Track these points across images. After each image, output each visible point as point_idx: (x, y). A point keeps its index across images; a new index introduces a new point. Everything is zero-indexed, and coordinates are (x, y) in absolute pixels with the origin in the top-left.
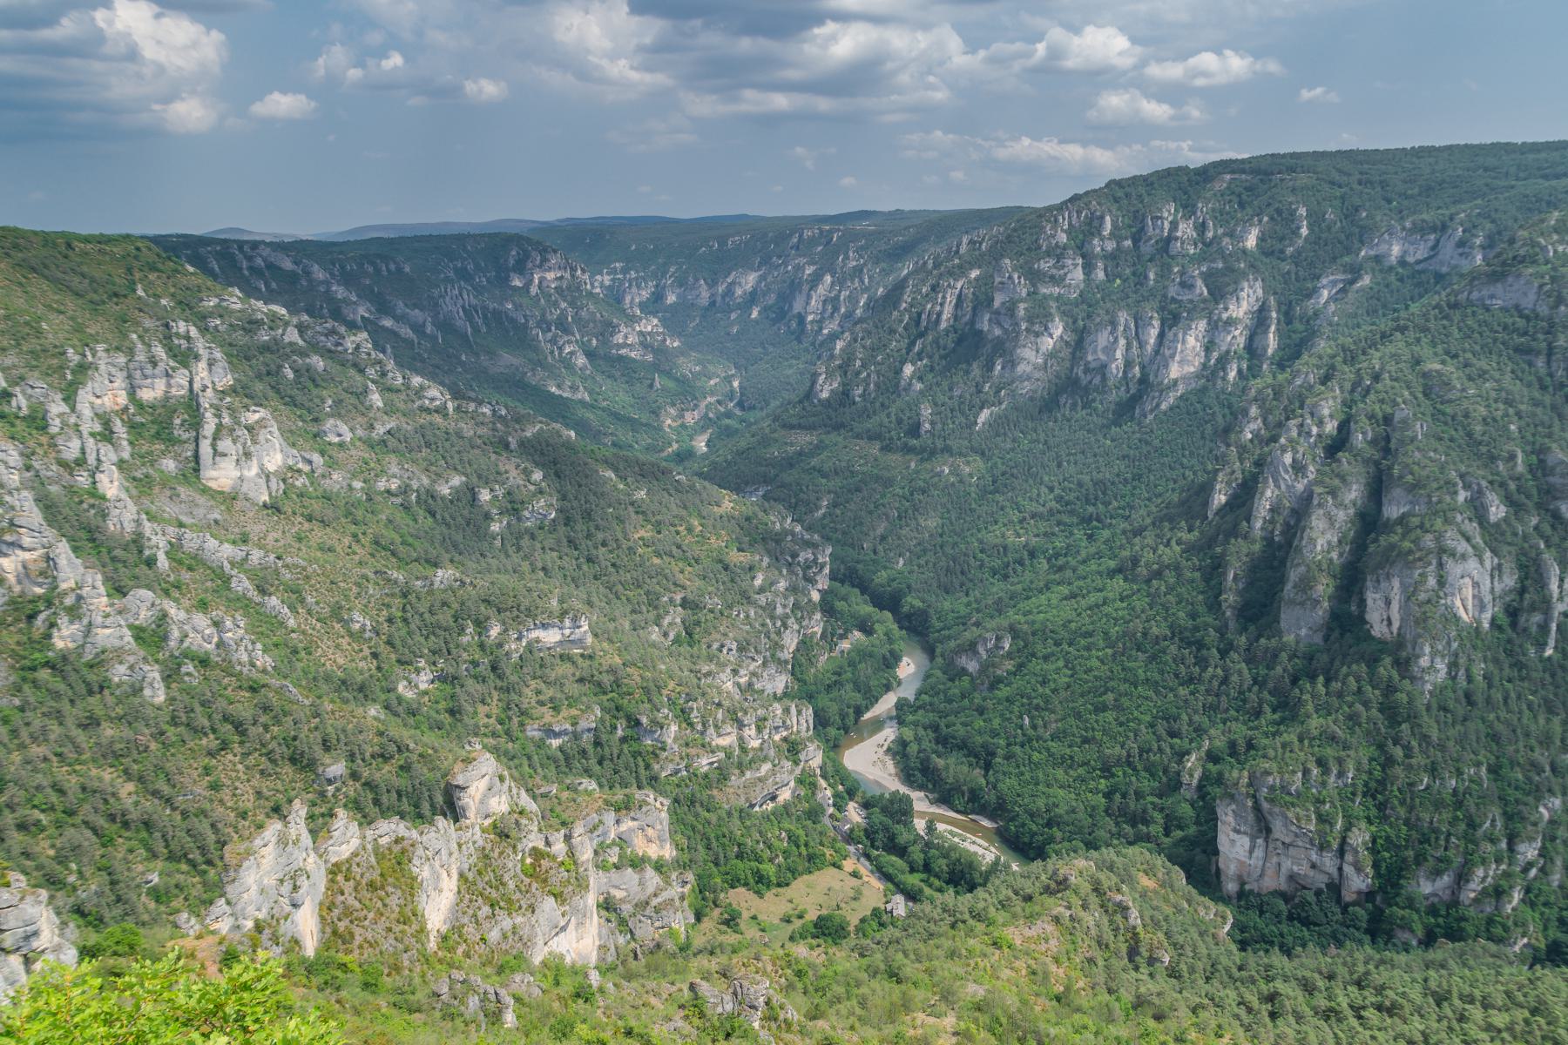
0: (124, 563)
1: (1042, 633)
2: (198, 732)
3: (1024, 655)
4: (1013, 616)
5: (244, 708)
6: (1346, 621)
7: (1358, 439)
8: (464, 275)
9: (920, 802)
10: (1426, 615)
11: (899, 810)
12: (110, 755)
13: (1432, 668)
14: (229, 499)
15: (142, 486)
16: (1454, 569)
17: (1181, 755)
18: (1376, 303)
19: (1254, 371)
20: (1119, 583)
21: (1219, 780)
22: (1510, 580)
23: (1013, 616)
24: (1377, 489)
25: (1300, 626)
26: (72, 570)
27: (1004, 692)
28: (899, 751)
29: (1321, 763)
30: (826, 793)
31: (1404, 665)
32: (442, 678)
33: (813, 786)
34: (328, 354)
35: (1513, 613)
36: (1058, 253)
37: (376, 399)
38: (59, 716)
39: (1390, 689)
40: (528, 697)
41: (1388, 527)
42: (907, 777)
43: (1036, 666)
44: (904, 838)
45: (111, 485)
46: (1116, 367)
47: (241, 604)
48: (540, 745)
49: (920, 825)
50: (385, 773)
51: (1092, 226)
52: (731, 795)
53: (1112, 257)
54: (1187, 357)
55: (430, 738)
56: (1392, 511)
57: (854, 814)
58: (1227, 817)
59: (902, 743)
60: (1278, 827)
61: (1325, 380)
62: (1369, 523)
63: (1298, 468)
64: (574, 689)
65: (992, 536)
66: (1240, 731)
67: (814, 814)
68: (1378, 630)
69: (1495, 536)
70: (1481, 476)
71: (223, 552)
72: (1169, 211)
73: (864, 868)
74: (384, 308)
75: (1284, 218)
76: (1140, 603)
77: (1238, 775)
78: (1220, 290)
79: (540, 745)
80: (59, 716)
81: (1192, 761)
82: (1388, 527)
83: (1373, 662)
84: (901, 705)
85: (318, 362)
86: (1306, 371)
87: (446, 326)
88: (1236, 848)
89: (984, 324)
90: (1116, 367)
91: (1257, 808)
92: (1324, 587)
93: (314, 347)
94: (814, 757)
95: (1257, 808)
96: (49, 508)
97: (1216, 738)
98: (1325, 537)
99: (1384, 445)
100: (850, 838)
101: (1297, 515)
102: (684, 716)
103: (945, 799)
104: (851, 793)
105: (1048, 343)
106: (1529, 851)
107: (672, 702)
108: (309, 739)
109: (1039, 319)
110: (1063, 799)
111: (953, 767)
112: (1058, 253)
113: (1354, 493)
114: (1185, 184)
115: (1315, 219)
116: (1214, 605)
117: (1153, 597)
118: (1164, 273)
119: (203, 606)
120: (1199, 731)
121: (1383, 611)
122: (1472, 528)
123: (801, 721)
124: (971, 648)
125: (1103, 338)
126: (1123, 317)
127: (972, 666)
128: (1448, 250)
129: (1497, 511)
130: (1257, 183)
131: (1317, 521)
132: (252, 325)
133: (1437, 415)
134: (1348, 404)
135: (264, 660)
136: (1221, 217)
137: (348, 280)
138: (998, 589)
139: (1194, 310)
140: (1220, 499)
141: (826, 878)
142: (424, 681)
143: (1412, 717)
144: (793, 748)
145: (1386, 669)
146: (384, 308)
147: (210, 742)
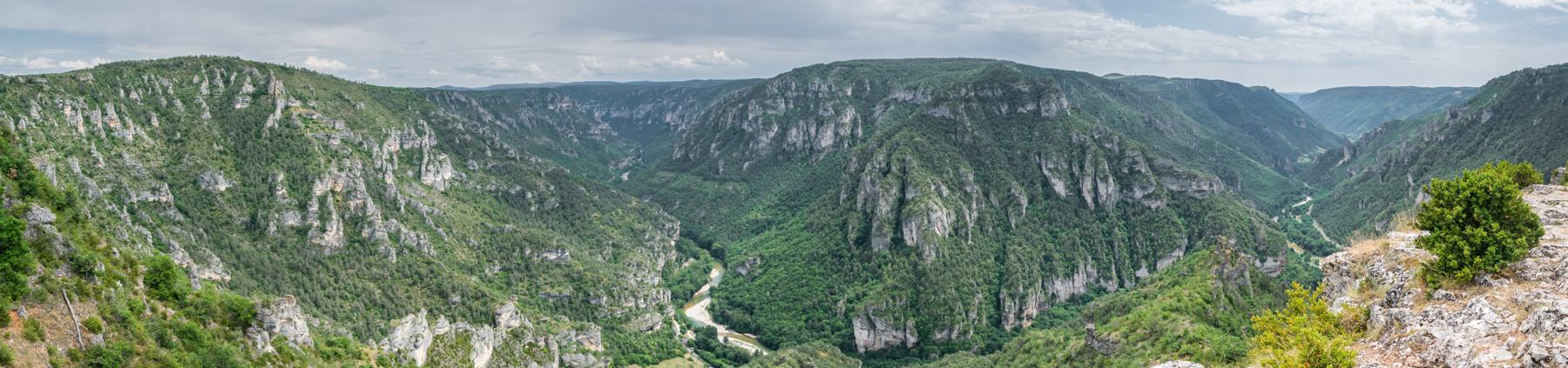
0: (390, 207)
1: (774, 256)
2: (406, 276)
3: (766, 266)
4: (761, 250)
5: (423, 271)
6: (898, 242)
7: (894, 169)
8: (530, 104)
9: (721, 330)
10: (925, 234)
11: (712, 333)
12: (374, 279)
13: (930, 257)
14: (430, 188)
15: (400, 180)
16: (934, 216)
17: (836, 302)
18: (896, 116)
19: (854, 144)
20: (805, 234)
21: (853, 310)
22: (953, 217)
23: (761, 250)
24: (903, 190)
25: (879, 244)
26: (372, 207)
27: (758, 282)
28: (711, 309)
29: (893, 297)
30: (677, 327)
31: (919, 255)
32: (504, 269)
33: (671, 324)
34: (473, 134)
35: (956, 230)
36: (774, 97)
37: (489, 153)
38: (359, 261)
39: (915, 265)
40: (541, 281)
41: (908, 202)
42: (715, 320)
43: (772, 270)
44: (713, 344)
45: (390, 179)
46: (799, 144)
47: (428, 229)
48: (545, 300)
49: (721, 339)
50: (476, 304)
51: (787, 87)
52: (632, 326)
53: (796, 99)
54: (827, 140)
55: (496, 292)
56: (909, 196)
57: (690, 335)
58: (857, 324)
59: (713, 305)
60: (879, 326)
61: (880, 146)
62: (902, 202)
63: (873, 182)
64: (561, 279)
65: (752, 216)
66: (860, 290)
67: (671, 336)
68: (909, 243)
69: (946, 201)
70: (938, 180)
71: (424, 208)
72: (817, 81)
73: (695, 357)
74: (498, 117)
75: (860, 83)
76: (815, 241)
77: (859, 306)
78: (838, 113)
79: (545, 300)
80: (359, 261)
81: (841, 304)
82: (908, 202)
83: (908, 255)
84: (712, 289)
85: (468, 137)
86: (872, 143)
87: (521, 125)
88: (862, 336)
89: (745, 126)
90: (799, 144)
91: (869, 319)
92: (887, 229)
93: (468, 131)
94: (671, 311)
95: (869, 319)
96: (368, 184)
97: (850, 293)
98: (884, 208)
99: (904, 171)
100: (689, 345)
101: (873, 199)
102: (610, 294)
103: (734, 326)
104: (689, 327)
105: (772, 134)
106: (973, 315)
107: (605, 288)
108: (447, 286)
109: (767, 125)
110: (787, 325)
111: (736, 314)
112: (774, 97)
113: (894, 191)
114: (823, 70)
115: (872, 84)
116: (845, 239)
117: (821, 238)
118: (817, 106)
119: (415, 228)
120: (843, 291)
121: (910, 236)
122: (938, 200)
123: (666, 297)
124: (743, 264)
125: (794, 132)
126: (801, 123)
127: (744, 272)
128: (919, 95)
129: (946, 192)
130: (849, 70)
131: (882, 202)
132: (446, 122)
133: (921, 158)
134: (889, 155)
135: (433, 252)
136: (837, 83)
137: (485, 106)
138: (756, 239)
139: (829, 119)
140: (843, 196)
141: (678, 360)
142: (497, 268)
143: (924, 274)
144: (661, 308)
145: (913, 257)
146: (498, 117)
147: (409, 281)
